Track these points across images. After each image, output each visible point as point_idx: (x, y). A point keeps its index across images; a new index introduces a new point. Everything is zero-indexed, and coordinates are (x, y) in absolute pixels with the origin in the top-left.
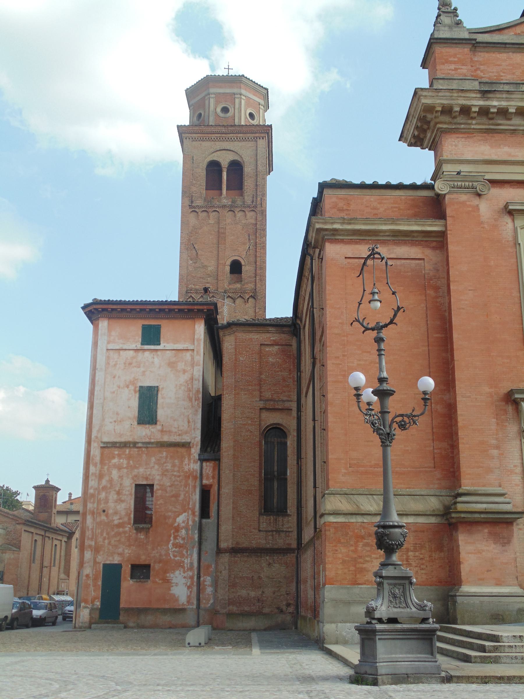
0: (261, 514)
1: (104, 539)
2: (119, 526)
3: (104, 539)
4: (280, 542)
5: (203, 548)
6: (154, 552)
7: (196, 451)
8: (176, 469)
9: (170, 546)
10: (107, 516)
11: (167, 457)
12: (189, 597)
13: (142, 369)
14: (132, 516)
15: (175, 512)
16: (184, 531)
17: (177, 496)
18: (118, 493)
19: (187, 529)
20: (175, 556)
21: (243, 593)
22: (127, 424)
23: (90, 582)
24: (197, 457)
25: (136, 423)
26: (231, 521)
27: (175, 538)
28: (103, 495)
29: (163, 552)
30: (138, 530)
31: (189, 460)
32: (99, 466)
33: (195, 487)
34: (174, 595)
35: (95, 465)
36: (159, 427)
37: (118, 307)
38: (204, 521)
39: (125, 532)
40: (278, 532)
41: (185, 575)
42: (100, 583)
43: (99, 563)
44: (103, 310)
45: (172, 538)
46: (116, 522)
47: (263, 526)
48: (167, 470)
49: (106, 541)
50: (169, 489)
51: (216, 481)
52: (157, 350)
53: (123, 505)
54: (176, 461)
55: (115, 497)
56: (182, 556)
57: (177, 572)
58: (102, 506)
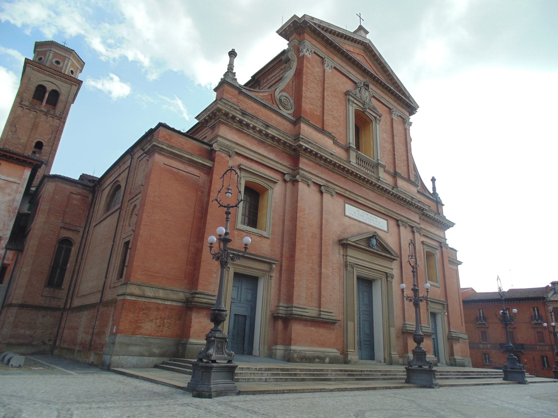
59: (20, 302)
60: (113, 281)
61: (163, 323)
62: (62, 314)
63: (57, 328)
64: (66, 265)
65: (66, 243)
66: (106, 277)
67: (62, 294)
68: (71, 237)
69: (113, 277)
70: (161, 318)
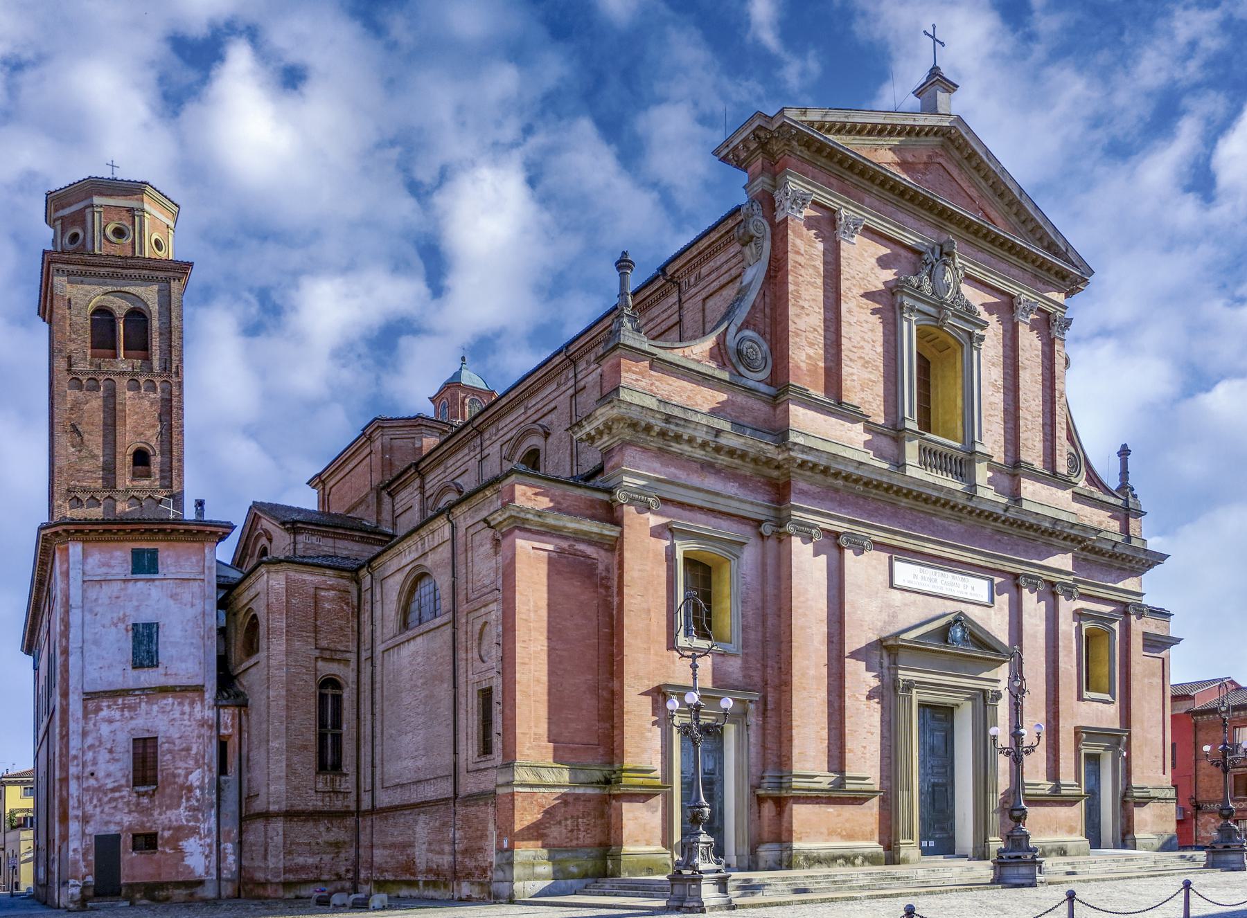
0: (317, 773)
4: (339, 804)
5: (222, 809)
6: (163, 817)
9: (182, 810)
11: (173, 704)
12: (207, 868)
15: (186, 768)
16: (198, 792)
19: (202, 788)
20: (188, 821)
23: (79, 857)
26: (283, 781)
27: (188, 799)
29: (173, 818)
34: (188, 867)
38: (223, 778)
40: (336, 793)
41: (202, 842)
42: (91, 857)
43: (90, 835)
45: (184, 800)
47: (320, 786)
48: (174, 719)
51: (236, 731)
59: (284, 807)
60: (470, 759)
61: (577, 826)
66: (455, 753)
67: (348, 784)
69: (470, 752)
70: (572, 817)
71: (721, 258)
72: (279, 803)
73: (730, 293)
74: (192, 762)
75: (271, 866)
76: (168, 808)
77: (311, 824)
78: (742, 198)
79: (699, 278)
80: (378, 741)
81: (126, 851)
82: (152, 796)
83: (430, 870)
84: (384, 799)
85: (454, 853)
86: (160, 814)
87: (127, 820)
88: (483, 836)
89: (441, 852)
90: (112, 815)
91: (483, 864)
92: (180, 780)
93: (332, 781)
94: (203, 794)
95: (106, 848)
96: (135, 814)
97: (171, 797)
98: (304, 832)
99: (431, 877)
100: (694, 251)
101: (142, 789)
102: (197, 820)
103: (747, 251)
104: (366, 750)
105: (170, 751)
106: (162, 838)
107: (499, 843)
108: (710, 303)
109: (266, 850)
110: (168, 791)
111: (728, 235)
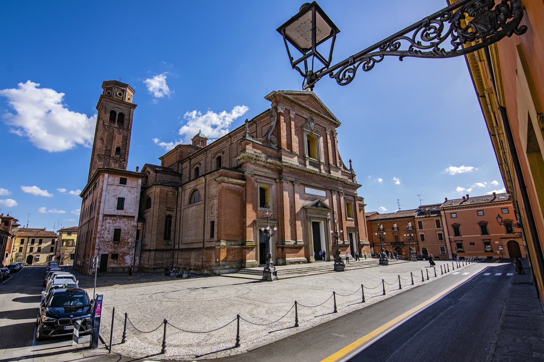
1: (102, 246)
2: (108, 242)
3: (102, 246)
4: (169, 247)
7: (136, 219)
8: (129, 224)
9: (126, 248)
10: (104, 239)
13: (120, 192)
14: (113, 239)
16: (130, 244)
17: (129, 233)
18: (108, 231)
19: (131, 243)
21: (158, 262)
22: (113, 210)
24: (136, 221)
25: (116, 209)
27: (127, 246)
28: (103, 232)
29: (123, 250)
30: (115, 244)
31: (134, 222)
32: (102, 222)
33: (135, 230)
35: (101, 222)
36: (124, 211)
37: (114, 171)
39: (110, 244)
40: (169, 245)
44: (108, 171)
46: (107, 241)
49: (103, 247)
50: (126, 230)
52: (125, 186)
53: (110, 235)
54: (130, 222)
55: (107, 232)
56: (129, 251)
57: (127, 256)
58: (102, 236)
59: (154, 248)
62: (173, 252)
63: (172, 259)
64: (171, 228)
65: (169, 217)
67: (172, 242)
68: (171, 214)
71: (266, 119)
72: (153, 247)
73: (268, 126)
74: (129, 236)
75: (150, 264)
76: (122, 248)
77: (161, 253)
78: (271, 107)
79: (261, 122)
80: (181, 232)
81: (109, 259)
82: (118, 244)
83: (195, 266)
84: (182, 247)
85: (203, 262)
86: (120, 249)
87: (111, 250)
88: (211, 258)
89: (199, 261)
90: (107, 248)
91: (211, 265)
92: (126, 240)
93: (168, 242)
94: (132, 244)
95: (104, 258)
96: (113, 249)
97: (123, 245)
98: (159, 254)
99: (195, 268)
100: (260, 117)
101: (115, 242)
102: (129, 251)
103: (272, 118)
104: (177, 234)
105: (124, 233)
106: (120, 255)
107: (216, 260)
108: (263, 128)
109: (149, 259)
110: (122, 243)
111: (267, 115)
